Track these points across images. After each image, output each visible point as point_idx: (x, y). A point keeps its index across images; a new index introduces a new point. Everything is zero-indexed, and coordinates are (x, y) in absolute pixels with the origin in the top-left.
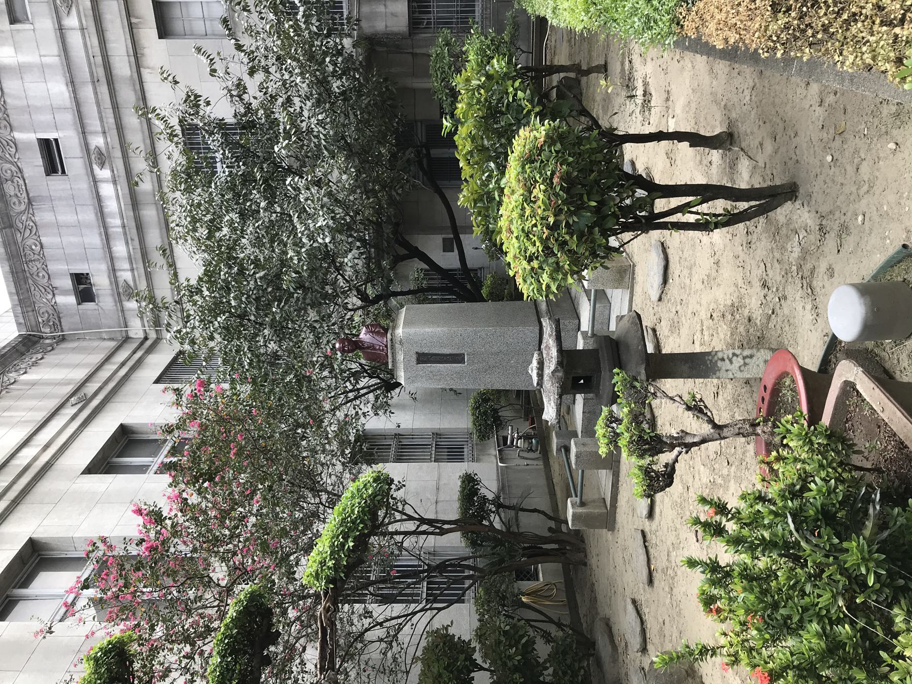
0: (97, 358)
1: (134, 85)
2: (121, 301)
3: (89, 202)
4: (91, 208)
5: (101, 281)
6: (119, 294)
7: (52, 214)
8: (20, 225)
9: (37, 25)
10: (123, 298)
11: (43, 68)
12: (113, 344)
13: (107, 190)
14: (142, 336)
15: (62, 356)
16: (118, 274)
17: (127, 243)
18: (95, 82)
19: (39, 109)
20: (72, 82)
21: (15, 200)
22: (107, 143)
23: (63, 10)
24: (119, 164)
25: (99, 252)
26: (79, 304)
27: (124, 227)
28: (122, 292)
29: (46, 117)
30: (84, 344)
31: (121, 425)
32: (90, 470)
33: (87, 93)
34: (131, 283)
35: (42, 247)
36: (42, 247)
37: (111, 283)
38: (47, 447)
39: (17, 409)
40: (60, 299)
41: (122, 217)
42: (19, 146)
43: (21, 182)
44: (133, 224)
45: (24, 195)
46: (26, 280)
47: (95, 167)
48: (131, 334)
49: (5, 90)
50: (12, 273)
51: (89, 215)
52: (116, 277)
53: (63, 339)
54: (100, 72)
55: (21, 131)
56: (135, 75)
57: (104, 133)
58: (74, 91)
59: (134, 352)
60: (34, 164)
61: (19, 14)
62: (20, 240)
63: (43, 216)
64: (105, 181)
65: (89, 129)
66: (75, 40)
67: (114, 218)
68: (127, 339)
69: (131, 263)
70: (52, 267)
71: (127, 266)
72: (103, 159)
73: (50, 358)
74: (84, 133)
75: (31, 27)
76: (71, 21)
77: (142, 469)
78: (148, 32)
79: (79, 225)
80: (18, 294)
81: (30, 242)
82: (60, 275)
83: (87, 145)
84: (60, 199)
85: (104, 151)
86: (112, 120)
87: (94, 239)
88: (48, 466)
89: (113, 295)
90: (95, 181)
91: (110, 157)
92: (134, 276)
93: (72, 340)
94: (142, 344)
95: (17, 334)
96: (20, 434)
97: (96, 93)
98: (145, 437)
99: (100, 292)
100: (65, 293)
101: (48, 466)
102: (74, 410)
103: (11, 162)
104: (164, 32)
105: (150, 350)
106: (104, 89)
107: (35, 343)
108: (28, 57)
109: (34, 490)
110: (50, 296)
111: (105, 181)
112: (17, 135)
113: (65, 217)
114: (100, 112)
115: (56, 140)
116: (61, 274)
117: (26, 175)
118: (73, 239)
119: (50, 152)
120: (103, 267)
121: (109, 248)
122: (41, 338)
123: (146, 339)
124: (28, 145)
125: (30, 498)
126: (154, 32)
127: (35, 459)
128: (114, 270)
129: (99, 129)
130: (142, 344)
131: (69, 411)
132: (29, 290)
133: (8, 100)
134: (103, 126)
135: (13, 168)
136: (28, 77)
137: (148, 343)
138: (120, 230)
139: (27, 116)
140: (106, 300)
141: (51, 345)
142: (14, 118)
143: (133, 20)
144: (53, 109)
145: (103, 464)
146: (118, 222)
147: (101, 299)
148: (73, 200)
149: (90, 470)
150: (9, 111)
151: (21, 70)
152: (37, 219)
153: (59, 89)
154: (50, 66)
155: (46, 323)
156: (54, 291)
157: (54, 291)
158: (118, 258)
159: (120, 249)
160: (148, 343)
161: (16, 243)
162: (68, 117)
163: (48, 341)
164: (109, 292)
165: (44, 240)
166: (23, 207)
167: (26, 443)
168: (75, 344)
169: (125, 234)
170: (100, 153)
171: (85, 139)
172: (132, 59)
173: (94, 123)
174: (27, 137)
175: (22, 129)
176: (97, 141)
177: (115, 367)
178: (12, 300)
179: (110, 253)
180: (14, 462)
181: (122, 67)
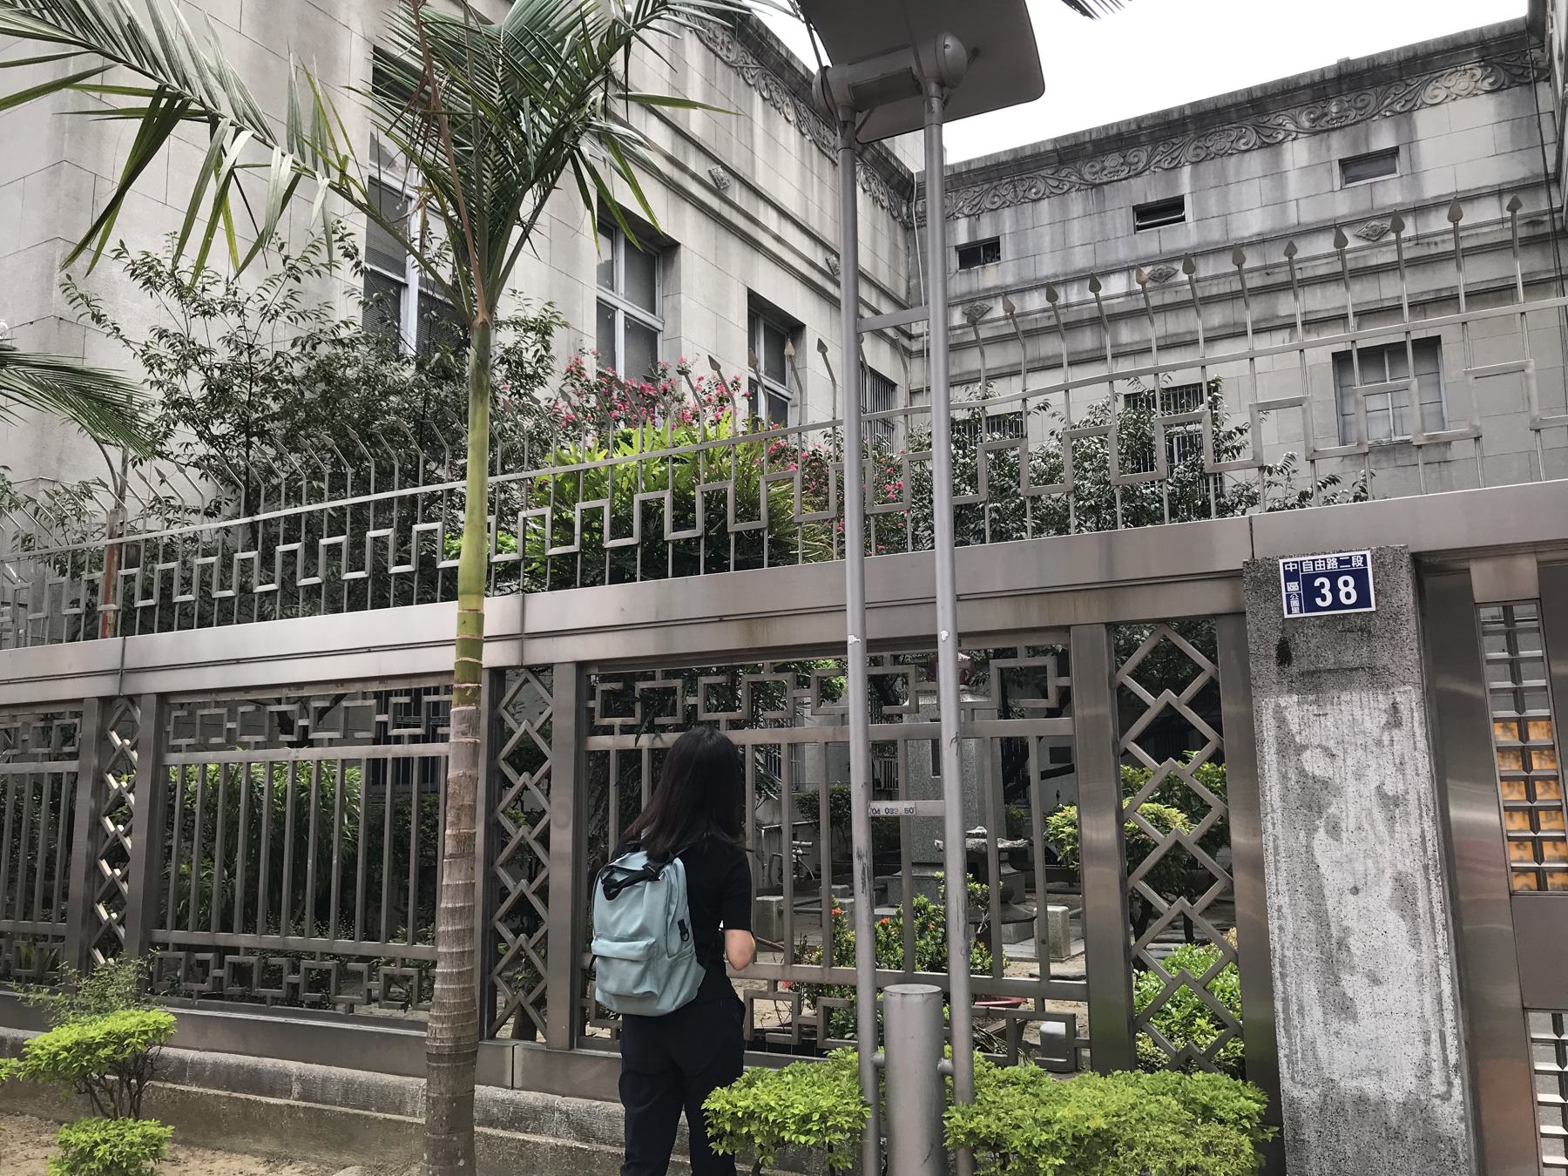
0: (884, 279)
1: (1265, 320)
2: (961, 303)
3: (1099, 261)
4: (1092, 264)
5: (990, 276)
6: (972, 300)
7: (1081, 213)
9: (1340, 196)
10: (967, 306)
11: (1281, 203)
12: (902, 294)
15: (885, 231)
17: (1044, 310)
19: (1224, 198)
20: (1264, 241)
21: (1098, 167)
23: (1363, 229)
25: (1029, 274)
26: (957, 248)
27: (1067, 306)
29: (1213, 206)
30: (902, 257)
31: (801, 327)
32: (753, 297)
34: (988, 317)
38: (778, 239)
39: (821, 191)
41: (1080, 304)
42: (1172, 173)
43: (1123, 175)
44: (1071, 319)
45: (1105, 179)
46: (988, 180)
49: (1247, 155)
50: (998, 164)
52: (996, 296)
55: (1192, 176)
56: (1278, 322)
60: (1148, 190)
61: (1352, 172)
62: (1043, 173)
63: (1077, 203)
70: (1007, 214)
73: (883, 217)
75: (1337, 187)
77: (753, 363)
79: (1066, 247)
80: (969, 171)
81: (1041, 186)
82: (997, 224)
84: (1102, 224)
86: (1214, 291)
88: (756, 245)
92: (999, 319)
95: (914, 171)
96: (792, 205)
99: (974, 276)
100: (972, 230)
101: (756, 245)
102: (821, 263)
103: (1148, 162)
105: (894, 344)
107: (902, 195)
108: (1294, 185)
109: (731, 237)
110: (966, 211)
113: (1077, 231)
115: (1183, 219)
116: (1002, 224)
117: (1132, 181)
118: (1047, 239)
120: (1010, 279)
122: (909, 201)
123: (911, 337)
124: (1175, 183)
125: (722, 233)
127: (765, 229)
131: (819, 257)
132: (975, 184)
133: (1233, 159)
134: (1205, 279)
135: (1141, 165)
136: (1266, 183)
139: (1213, 182)
140: (962, 283)
141: (900, 215)
142: (1209, 168)
144: (1225, 216)
145: (761, 311)
147: (965, 277)
148: (1099, 241)
149: (753, 297)
150: (1218, 161)
151: (1276, 174)
152: (1074, 194)
153: (1253, 223)
154: (1284, 212)
156: (975, 216)
157: (975, 216)
158: (1022, 299)
160: (905, 342)
161: (1039, 168)
162: (1215, 234)
163: (904, 209)
164: (975, 287)
165: (1045, 203)
166: (1088, 177)
167: (783, 213)
168: (901, 246)
170: (1169, 276)
174: (1185, 182)
177: (874, 304)
178: (960, 164)
179: (1031, 289)
180: (761, 204)
181: (1287, 306)
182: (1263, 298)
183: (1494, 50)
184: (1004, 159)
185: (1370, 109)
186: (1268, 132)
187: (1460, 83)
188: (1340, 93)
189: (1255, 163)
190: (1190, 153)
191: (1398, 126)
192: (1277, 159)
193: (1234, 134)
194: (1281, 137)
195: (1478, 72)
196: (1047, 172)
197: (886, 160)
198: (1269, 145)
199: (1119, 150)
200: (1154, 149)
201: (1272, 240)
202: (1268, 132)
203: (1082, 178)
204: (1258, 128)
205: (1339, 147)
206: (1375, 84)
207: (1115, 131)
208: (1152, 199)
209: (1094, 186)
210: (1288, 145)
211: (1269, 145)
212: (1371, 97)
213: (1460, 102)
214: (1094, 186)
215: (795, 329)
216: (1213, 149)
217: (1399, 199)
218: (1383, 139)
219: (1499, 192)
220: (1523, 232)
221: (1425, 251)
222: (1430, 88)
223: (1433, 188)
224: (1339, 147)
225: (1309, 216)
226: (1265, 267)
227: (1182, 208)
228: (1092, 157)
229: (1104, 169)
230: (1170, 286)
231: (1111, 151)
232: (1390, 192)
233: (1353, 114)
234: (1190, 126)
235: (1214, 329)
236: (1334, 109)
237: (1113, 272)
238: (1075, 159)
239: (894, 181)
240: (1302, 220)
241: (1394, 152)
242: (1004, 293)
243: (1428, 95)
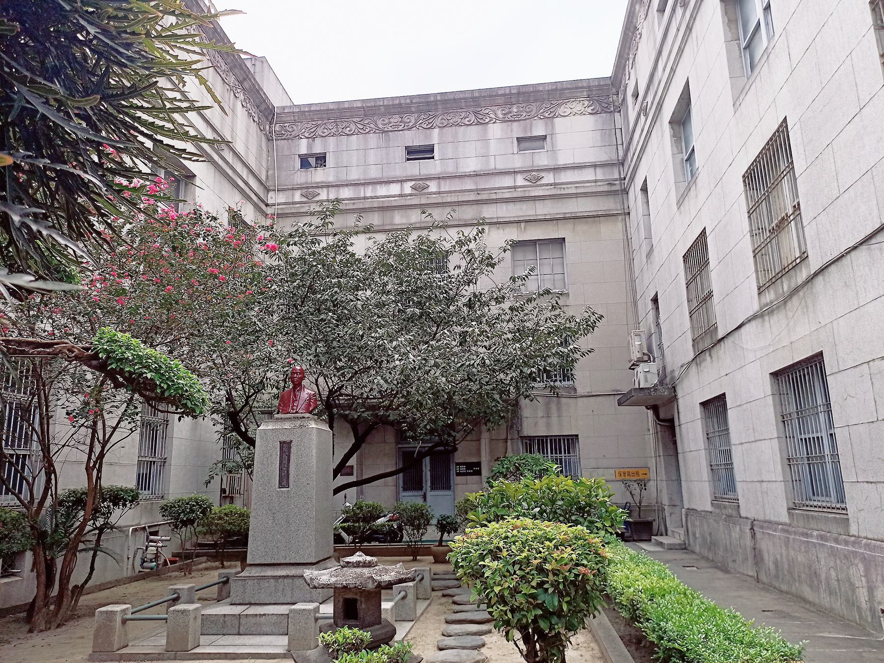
3: (384, 175)
4: (380, 176)
5: (319, 175)
6: (307, 188)
8: (366, 122)
12: (263, 178)
13: (395, 189)
16: (325, 190)
17: (351, 199)
18: (478, 191)
20: (477, 175)
21: (387, 121)
24: (415, 201)
25: (343, 177)
27: (365, 198)
28: (310, 191)
30: (265, 155)
33: (469, 185)
35: (348, 135)
36: (348, 135)
40: (304, 143)
41: (372, 198)
42: (428, 131)
43: (400, 128)
46: (322, 119)
47: (413, 183)
48: (271, 194)
51: (374, 173)
52: (322, 187)
53: (269, 140)
54: (484, 196)
57: (439, 193)
58: (470, 176)
60: (416, 139)
61: (523, 145)
62: (355, 120)
63: (373, 140)
64: (402, 188)
65: (442, 182)
66: (507, 181)
67: (372, 191)
68: (267, 190)
70: (331, 140)
71: (332, 197)
74: (439, 178)
76: (520, 181)
78: (515, 234)
81: (353, 127)
83: (430, 179)
85: (425, 191)
86: (449, 200)
87: (354, 175)
89: (306, 183)
90: (402, 181)
93: (267, 146)
94: (263, 201)
100: (310, 146)
104: (516, 245)
106: (472, 197)
111: (402, 188)
112: (436, 131)
114: (455, 191)
115: (433, 158)
119: (423, 153)
120: (331, 179)
121: (347, 185)
123: (267, 205)
126: (516, 238)
128: (328, 187)
129: (442, 190)
130: (263, 201)
135: (411, 124)
138: (362, 195)
140: (302, 177)
141: (264, 129)
143: (523, 225)
151: (485, 140)
153: (471, 165)
158: (339, 190)
159: (346, 193)
162: (450, 169)
163: (268, 127)
164: (309, 181)
166: (381, 126)
168: (264, 149)
169: (359, 199)
171: (434, 178)
173: (446, 186)
174: (435, 137)
175: (441, 135)
176: (433, 187)
181: (489, 212)
182: (475, 207)
183: (594, 93)
184: (331, 107)
185: (533, 113)
186: (481, 117)
187: (578, 107)
188: (518, 102)
189: (473, 132)
190: (438, 122)
191: (546, 125)
192: (485, 131)
193: (463, 115)
194: (487, 120)
195: (586, 103)
197: (258, 91)
201: (480, 175)
202: (481, 117)
203: (376, 125)
204: (476, 113)
205: (517, 130)
206: (535, 101)
207: (397, 102)
208: (416, 143)
210: (490, 125)
212: (534, 107)
213: (577, 116)
217: (546, 163)
218: (539, 129)
219: (595, 166)
220: (606, 188)
221: (559, 192)
222: (563, 107)
223: (562, 161)
224: (517, 130)
225: (501, 165)
226: (477, 190)
227: (432, 151)
228: (384, 115)
232: (542, 159)
233: (524, 114)
234: (440, 106)
236: (515, 110)
237: (393, 182)
238: (373, 115)
239: (263, 107)
240: (497, 167)
241: (544, 138)
242: (328, 186)
243: (561, 110)
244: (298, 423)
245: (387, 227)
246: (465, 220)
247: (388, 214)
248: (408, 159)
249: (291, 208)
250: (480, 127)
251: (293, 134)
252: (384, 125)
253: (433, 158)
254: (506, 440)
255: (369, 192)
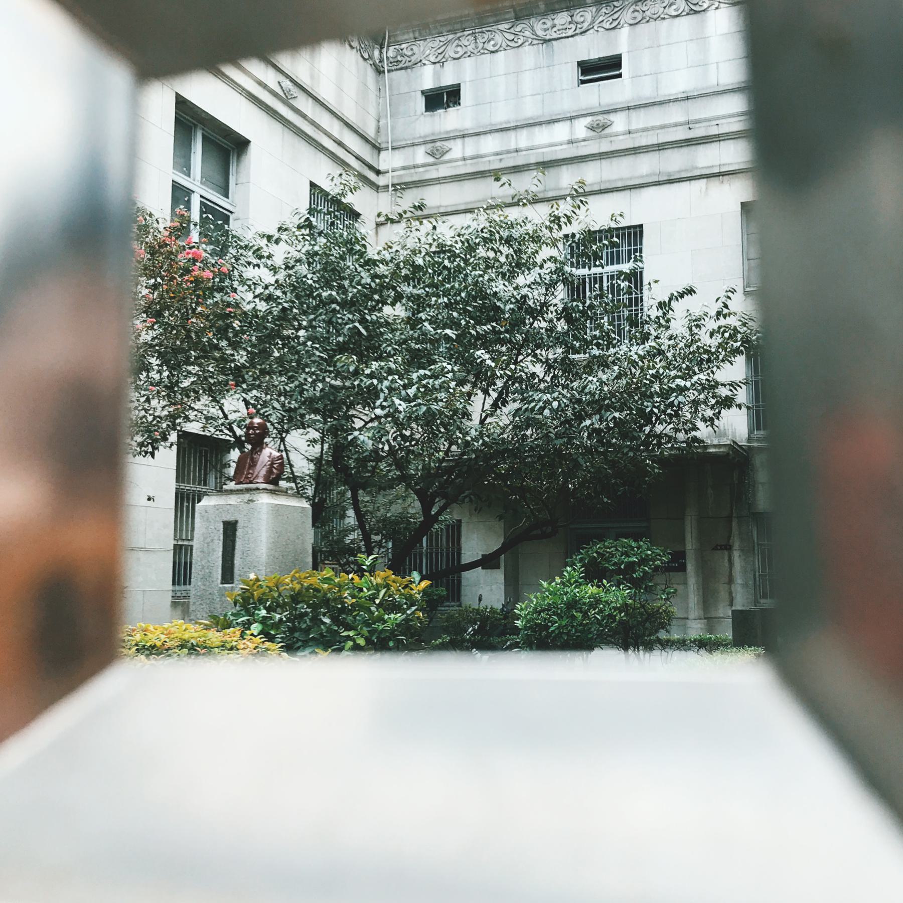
1: (686, 170)
2: (425, 143)
5: (449, 119)
6: (433, 141)
8: (518, 28)
10: (430, 146)
11: (705, 65)
13: (561, 132)
14: (382, 168)
16: (459, 142)
18: (689, 124)
20: (688, 98)
21: (549, 23)
22: (617, 135)
26: (423, 92)
28: (436, 147)
31: (248, 142)
33: (675, 114)
34: (447, 157)
35: (492, 52)
36: (492, 52)
37: (447, 132)
43: (570, 33)
46: (453, 32)
49: (678, 19)
51: (531, 110)
52: (455, 138)
53: (379, 72)
58: (676, 100)
59: (358, 158)
60: (593, 47)
63: (530, 55)
68: (378, 149)
69: (473, 158)
70: (467, 62)
71: (469, 152)
72: (598, 129)
74: (629, 108)
85: (607, 131)
86: (644, 142)
87: (502, 115)
89: (433, 134)
91: (600, 137)
92: (456, 160)
97: (676, 125)
98: (233, 169)
99: (437, 118)
100: (437, 76)
103: (593, 22)
106: (681, 134)
110: (433, 59)
112: (625, 31)
113: (529, 82)
114: (653, 128)
122: (382, 47)
123: (378, 173)
128: (463, 136)
129: (633, 127)
133: (665, 22)
134: (637, 131)
135: (585, 25)
137: (372, 176)
141: (370, 57)
146: (523, 144)
147: (428, 119)
150: (652, 23)
151: (701, 39)
155: (400, 52)
157: (440, 63)
159: (490, 144)
160: (372, 176)
162: (647, 93)
165: (501, 55)
166: (540, 33)
169: (508, 152)
170: (604, 127)
171: (622, 109)
172: (716, 170)
173: (640, 120)
174: (621, 42)
176: (619, 123)
179: (485, 133)
182: (685, 151)
190: (627, 16)
196: (504, 26)
198: (696, 12)
199: (568, 9)
200: (598, 11)
209: (545, 41)
211: (696, 12)
214: (545, 41)
215: (241, 145)
216: (648, 13)
229: (554, 26)
230: (606, 136)
231: (561, 10)
235: (642, 177)
240: (721, 82)
244: (247, 496)
245: (550, 194)
246: (669, 174)
247: (552, 172)
248: (583, 82)
249: (411, 175)
250: (695, 16)
251: (413, 59)
252: (546, 30)
253: (620, 76)
254: (729, 519)
255: (522, 139)
